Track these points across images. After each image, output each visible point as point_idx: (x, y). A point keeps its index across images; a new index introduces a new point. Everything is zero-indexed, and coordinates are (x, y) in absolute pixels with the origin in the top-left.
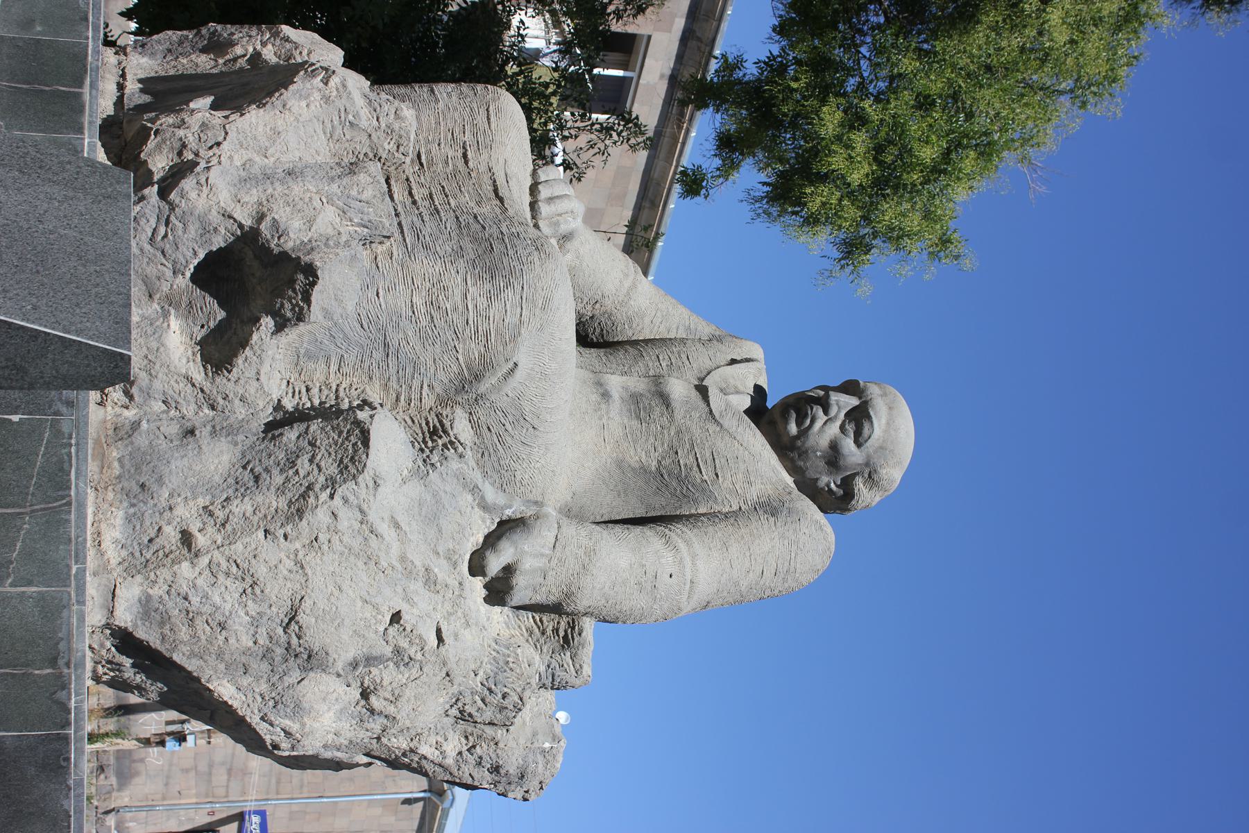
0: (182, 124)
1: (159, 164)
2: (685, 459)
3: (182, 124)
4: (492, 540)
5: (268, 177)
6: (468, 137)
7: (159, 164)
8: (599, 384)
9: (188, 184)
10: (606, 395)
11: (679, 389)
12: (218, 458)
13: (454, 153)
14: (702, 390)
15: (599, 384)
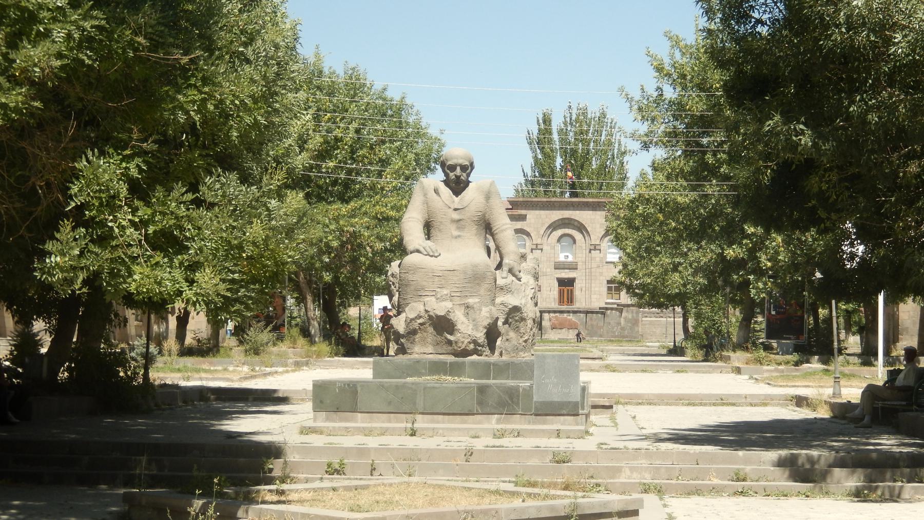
0: (463, 342)
1: (472, 346)
2: (476, 219)
3: (463, 342)
4: (514, 275)
5: (474, 325)
6: (431, 274)
7: (472, 346)
8: (456, 237)
9: (479, 341)
10: (459, 236)
11: (456, 216)
12: (512, 334)
13: (437, 279)
14: (456, 210)
15: (456, 237)
